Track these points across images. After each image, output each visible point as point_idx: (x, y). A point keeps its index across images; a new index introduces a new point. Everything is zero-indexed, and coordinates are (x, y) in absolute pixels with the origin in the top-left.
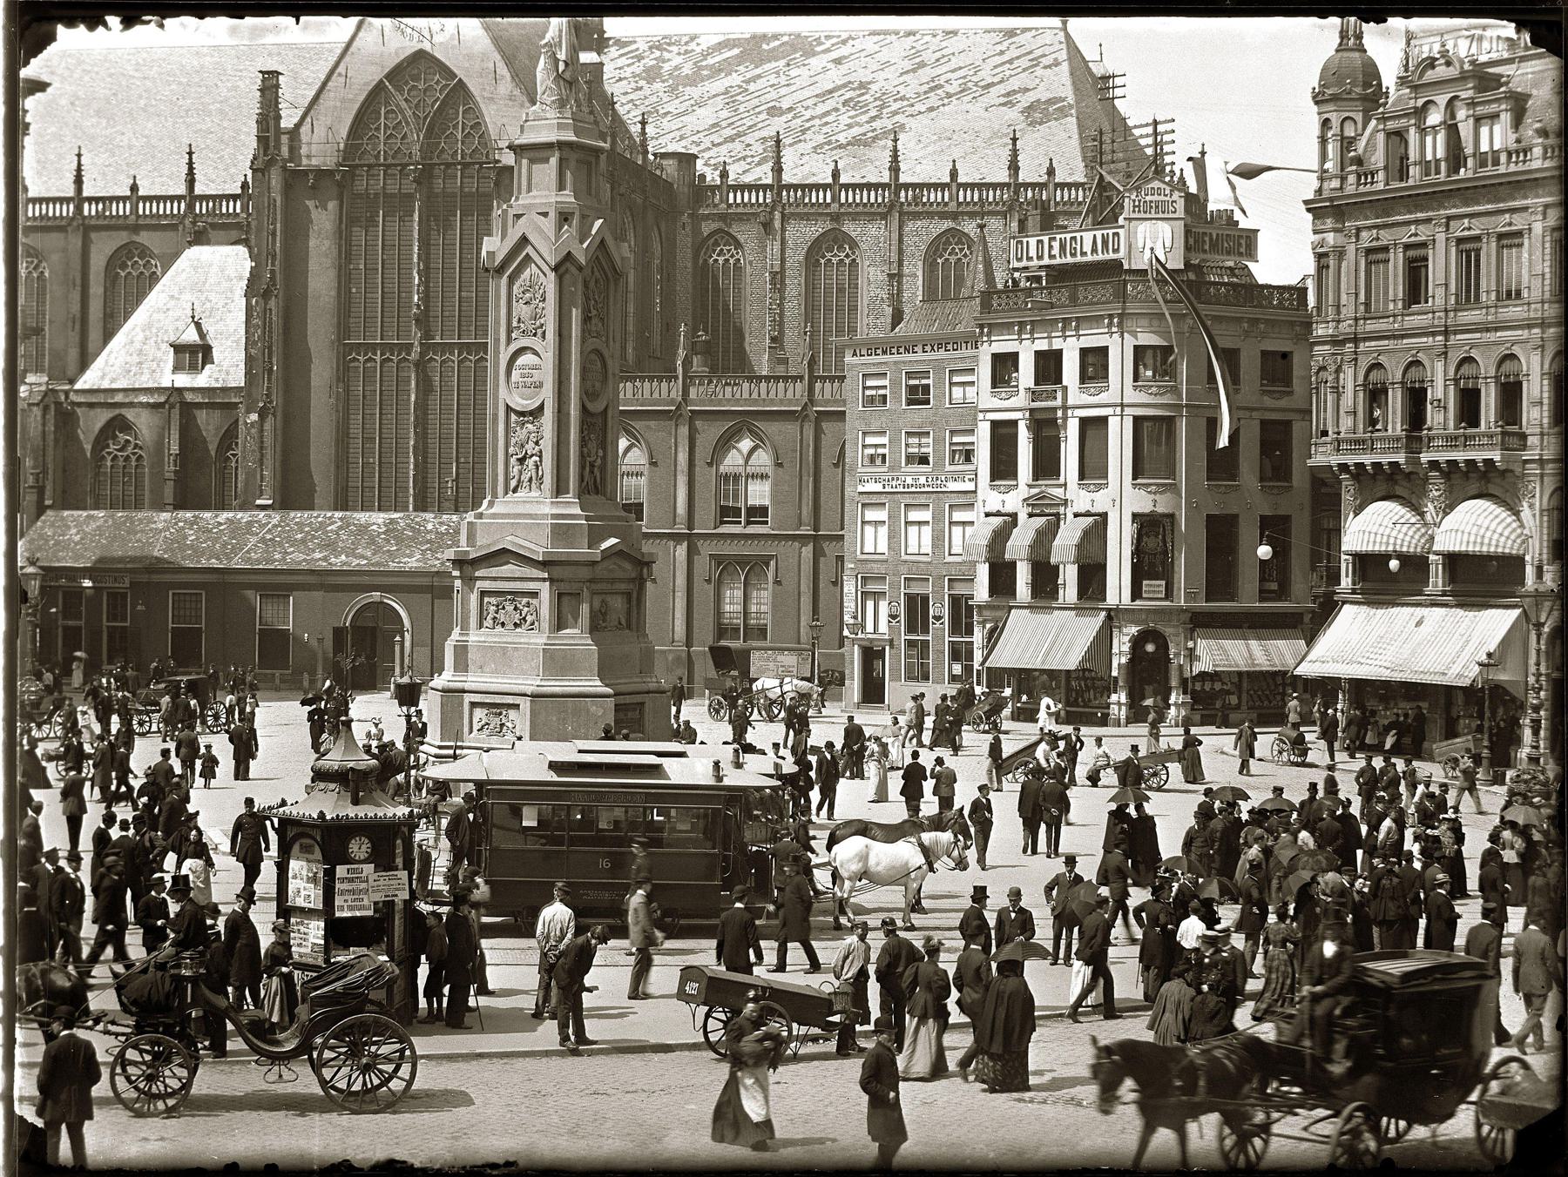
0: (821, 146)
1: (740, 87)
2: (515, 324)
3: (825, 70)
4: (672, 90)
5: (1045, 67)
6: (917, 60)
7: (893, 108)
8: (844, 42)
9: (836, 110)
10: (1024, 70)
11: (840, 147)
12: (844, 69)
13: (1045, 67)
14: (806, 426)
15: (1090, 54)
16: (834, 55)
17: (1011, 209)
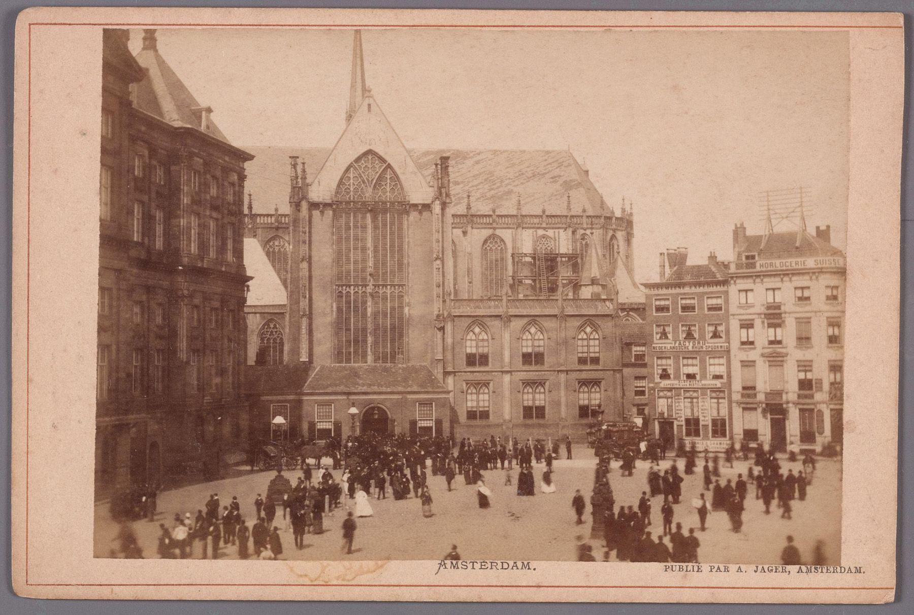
8: (479, 154)
9: (482, 183)
10: (557, 168)
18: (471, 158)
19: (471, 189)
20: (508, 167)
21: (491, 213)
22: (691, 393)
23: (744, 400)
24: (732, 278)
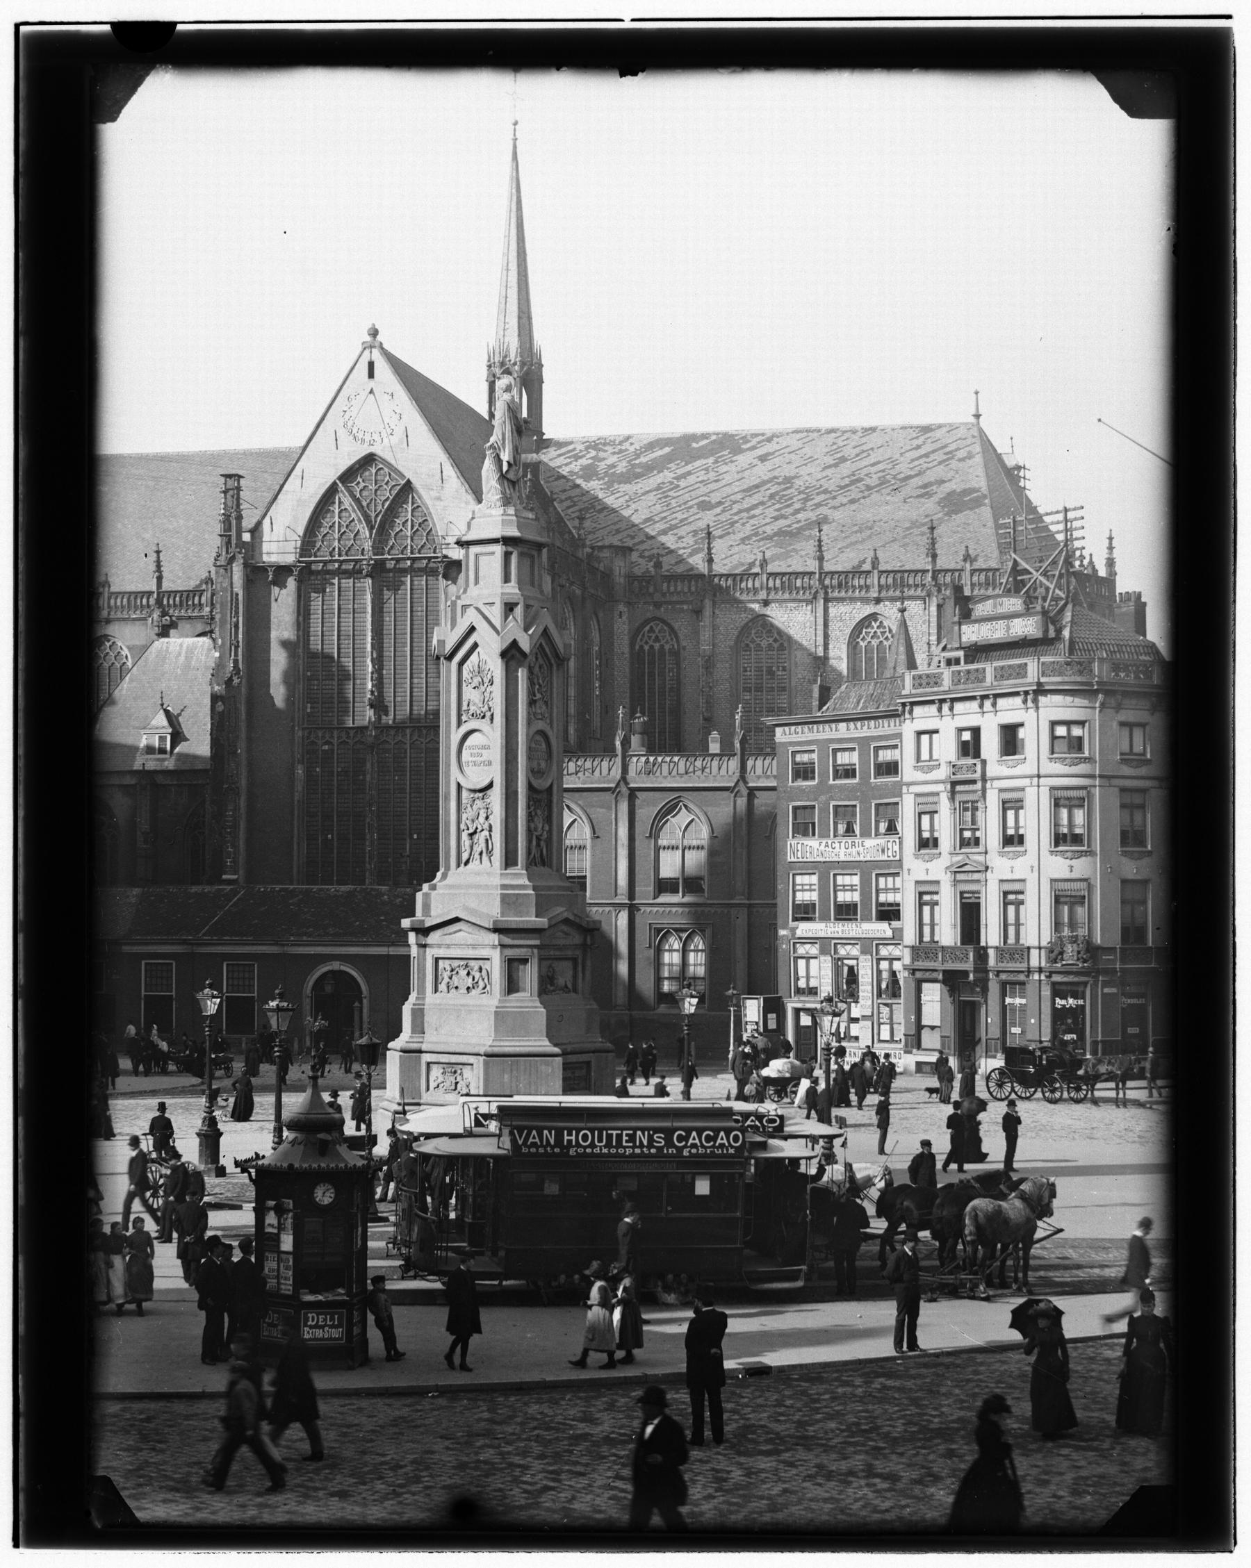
0: (748, 538)
1: (671, 483)
2: (465, 707)
3: (752, 466)
4: (609, 485)
5: (960, 460)
6: (839, 455)
7: (816, 501)
8: (769, 440)
9: (762, 503)
10: (940, 463)
11: (770, 538)
12: (769, 465)
13: (960, 460)
15: (1001, 447)
16: (760, 452)
18: (754, 448)
19: (736, 518)
20: (830, 467)
22: (848, 947)
24: (904, 704)
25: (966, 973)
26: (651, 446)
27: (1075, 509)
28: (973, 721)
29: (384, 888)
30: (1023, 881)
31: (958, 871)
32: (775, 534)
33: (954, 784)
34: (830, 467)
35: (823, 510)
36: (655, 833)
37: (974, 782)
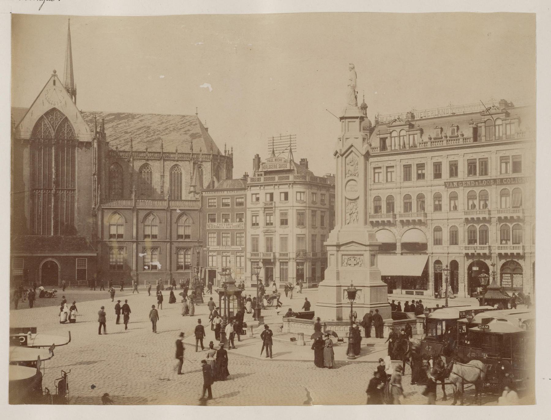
0: (140, 142)
1: (116, 126)
2: (347, 172)
3: (138, 123)
5: (194, 125)
6: (161, 121)
8: (142, 116)
11: (145, 142)
12: (143, 123)
14: (168, 213)
15: (203, 123)
16: (140, 119)
17: (191, 160)
18: (138, 118)
20: (159, 124)
21: (145, 151)
22: (226, 253)
23: (253, 257)
24: (248, 186)
25: (270, 260)
26: (109, 115)
27: (293, 135)
28: (271, 191)
29: (63, 236)
30: (259, 235)
31: (266, 232)
32: (147, 142)
33: (265, 208)
34: (159, 124)
35: (159, 136)
36: (143, 221)
37: (272, 208)
